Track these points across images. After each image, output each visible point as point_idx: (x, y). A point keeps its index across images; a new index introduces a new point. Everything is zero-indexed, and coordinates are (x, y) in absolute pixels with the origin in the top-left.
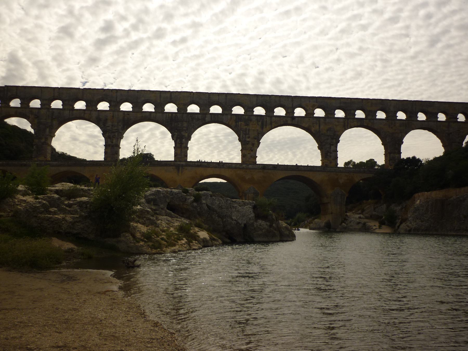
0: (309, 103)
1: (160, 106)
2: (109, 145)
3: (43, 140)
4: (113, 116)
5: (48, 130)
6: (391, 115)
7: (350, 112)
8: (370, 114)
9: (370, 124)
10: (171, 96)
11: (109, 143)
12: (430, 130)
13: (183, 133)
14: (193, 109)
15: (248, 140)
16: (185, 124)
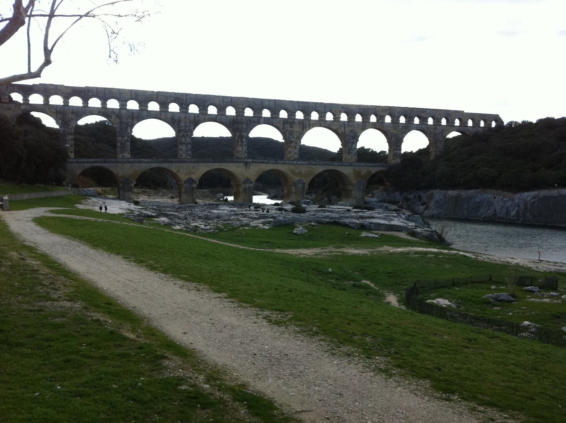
0: (336, 109)
1: (221, 109)
2: (184, 143)
3: (126, 138)
4: (185, 118)
5: (129, 128)
6: (395, 119)
7: (366, 117)
8: (381, 118)
9: (380, 126)
10: (231, 101)
11: (184, 141)
12: (421, 131)
13: (243, 134)
14: (249, 112)
15: (292, 139)
16: (244, 126)
